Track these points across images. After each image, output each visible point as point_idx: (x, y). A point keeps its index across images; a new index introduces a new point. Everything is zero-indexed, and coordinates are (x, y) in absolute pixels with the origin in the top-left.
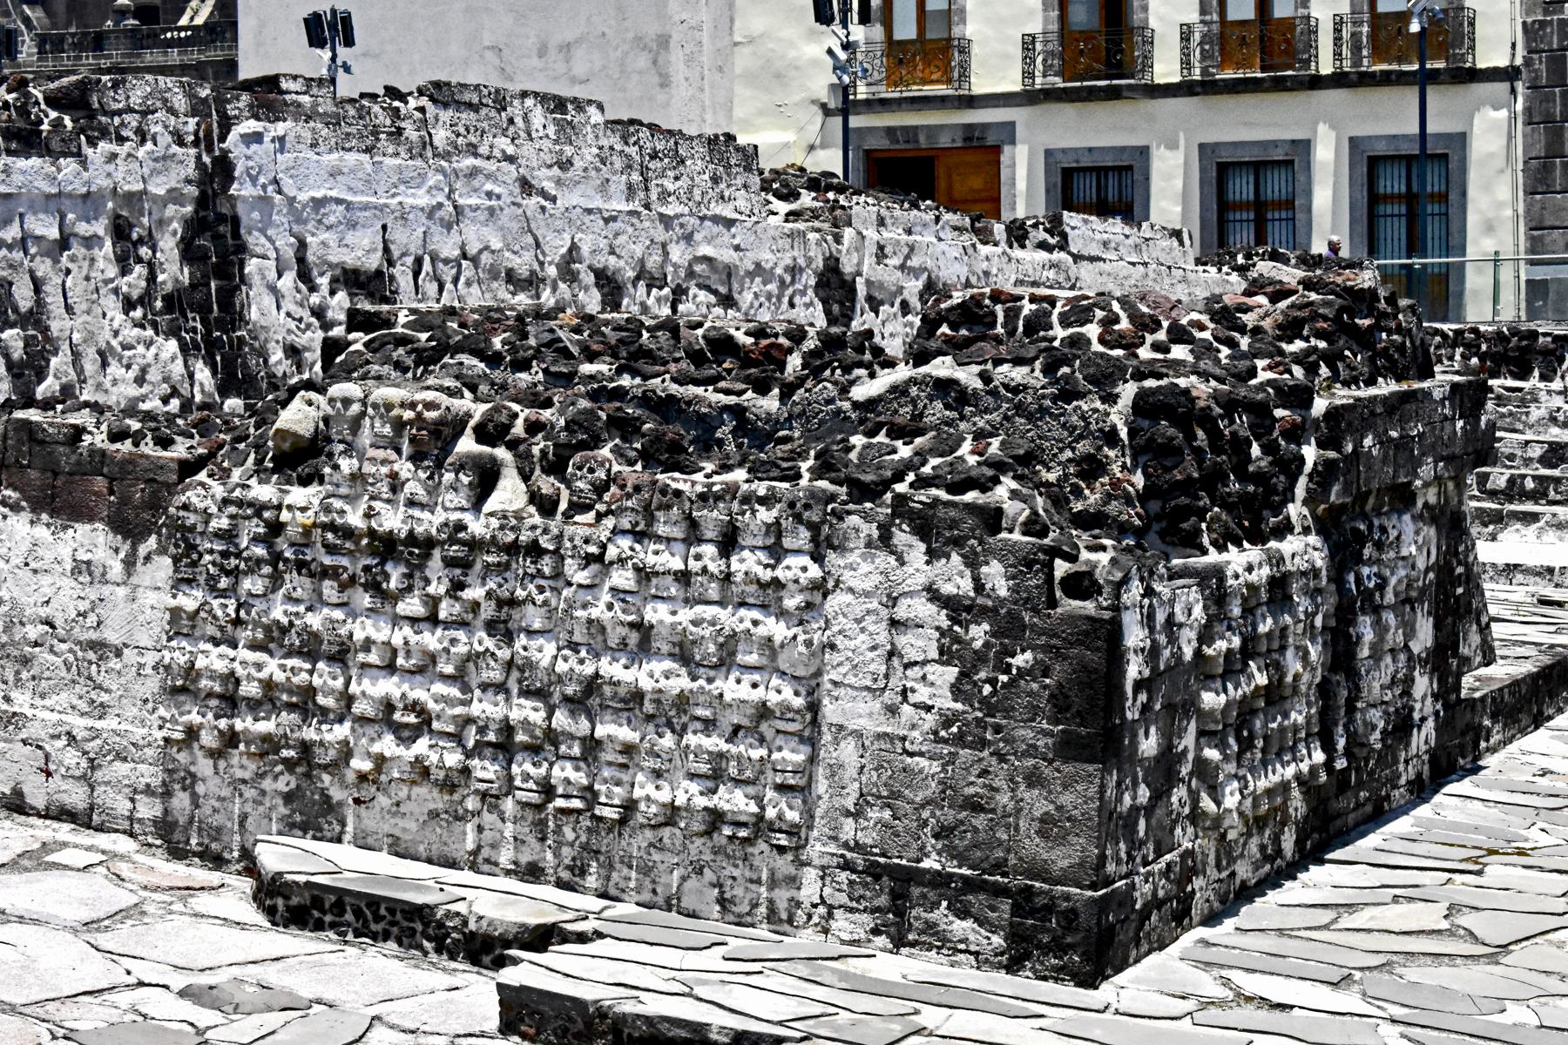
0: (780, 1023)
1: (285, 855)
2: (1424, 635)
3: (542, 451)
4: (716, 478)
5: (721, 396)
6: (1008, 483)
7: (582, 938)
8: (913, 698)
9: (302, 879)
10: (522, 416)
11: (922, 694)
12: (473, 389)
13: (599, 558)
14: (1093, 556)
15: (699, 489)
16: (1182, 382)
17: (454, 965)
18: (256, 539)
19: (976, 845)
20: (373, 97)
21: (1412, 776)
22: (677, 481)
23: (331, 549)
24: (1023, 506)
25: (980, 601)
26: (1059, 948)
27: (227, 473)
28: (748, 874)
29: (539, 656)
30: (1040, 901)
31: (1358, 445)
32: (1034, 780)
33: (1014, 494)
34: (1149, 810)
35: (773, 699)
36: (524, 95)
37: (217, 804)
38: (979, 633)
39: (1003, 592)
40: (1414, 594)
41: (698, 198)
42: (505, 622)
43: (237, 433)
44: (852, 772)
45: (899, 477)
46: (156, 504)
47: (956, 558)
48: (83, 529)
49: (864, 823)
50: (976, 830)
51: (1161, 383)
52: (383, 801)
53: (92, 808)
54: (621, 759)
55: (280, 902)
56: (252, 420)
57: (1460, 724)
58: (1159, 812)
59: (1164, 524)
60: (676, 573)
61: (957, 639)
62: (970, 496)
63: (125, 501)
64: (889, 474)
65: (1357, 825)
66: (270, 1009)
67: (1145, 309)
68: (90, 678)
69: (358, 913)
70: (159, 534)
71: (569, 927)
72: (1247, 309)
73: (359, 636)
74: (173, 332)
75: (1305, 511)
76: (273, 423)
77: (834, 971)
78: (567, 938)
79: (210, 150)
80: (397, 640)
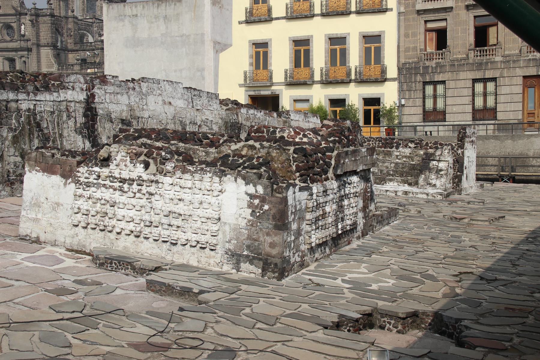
0: (210, 288)
1: (100, 251)
2: (361, 204)
4: (198, 166)
5: (202, 149)
6: (264, 168)
7: (166, 270)
8: (241, 216)
9: (103, 256)
10: (155, 152)
11: (243, 216)
12: (145, 146)
13: (172, 184)
14: (282, 185)
15: (195, 169)
16: (304, 147)
17: (137, 276)
18: (94, 179)
19: (255, 249)
20: (129, 81)
21: (357, 236)
22: (190, 168)
24: (266, 173)
25: (257, 194)
26: (274, 272)
27: (88, 164)
28: (204, 255)
29: (158, 206)
30: (269, 261)
31: (344, 161)
32: (268, 234)
33: (265, 171)
34: (294, 241)
35: (210, 216)
36: (164, 81)
37: (84, 240)
38: (257, 202)
39: (262, 192)
40: (357, 195)
41: (205, 105)
42: (151, 199)
44: (228, 232)
45: (239, 167)
46: (71, 171)
47: (251, 185)
48: (54, 177)
49: (230, 244)
50: (255, 246)
51: (300, 146)
52: (122, 239)
53: (55, 240)
54: (176, 229)
55: (98, 261)
57: (369, 225)
58: (297, 242)
59: (300, 178)
61: (251, 203)
62: (255, 171)
63: (64, 170)
64: (237, 166)
65: (344, 246)
66: (93, 285)
67: (297, 130)
68: (56, 211)
69: (115, 264)
70: (72, 178)
71: (163, 267)
72: (321, 131)
73: (117, 201)
74: (81, 133)
75: (332, 175)
77: (223, 277)
78: (163, 269)
79: (90, 92)
80: (126, 203)
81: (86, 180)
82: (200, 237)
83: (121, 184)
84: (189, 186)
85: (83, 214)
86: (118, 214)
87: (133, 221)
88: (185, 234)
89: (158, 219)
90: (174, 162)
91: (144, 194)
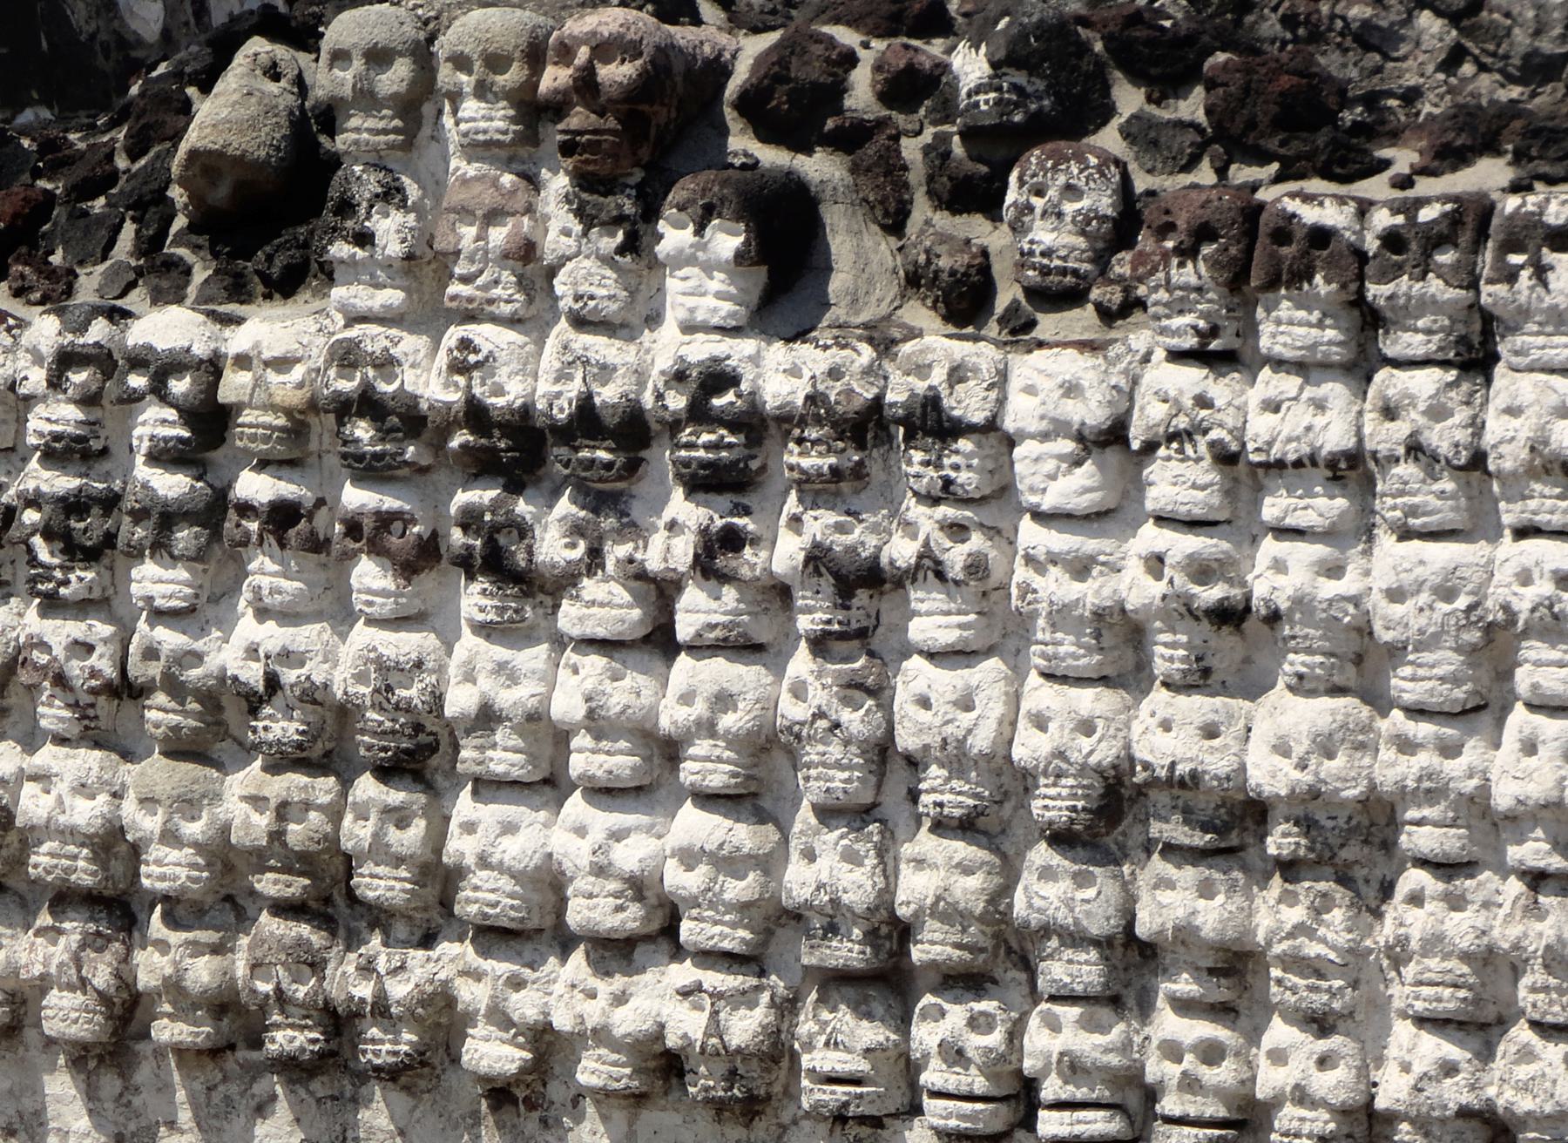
3: (927, 150)
4: (1424, 186)
10: (867, 58)
13: (1114, 435)
15: (1382, 219)
18: (163, 456)
23: (370, 470)
43: (80, 172)
56: (121, 134)
60: (1332, 463)
73: (460, 701)
76: (177, 136)
80: (567, 705)
81: (62, 483)
82: (1523, 1072)
83: (483, 495)
84: (1334, 436)
85: (64, 899)
86: (484, 862)
87: (670, 930)
88: (1335, 1042)
89: (975, 882)
90: (1108, 160)
91: (780, 593)
